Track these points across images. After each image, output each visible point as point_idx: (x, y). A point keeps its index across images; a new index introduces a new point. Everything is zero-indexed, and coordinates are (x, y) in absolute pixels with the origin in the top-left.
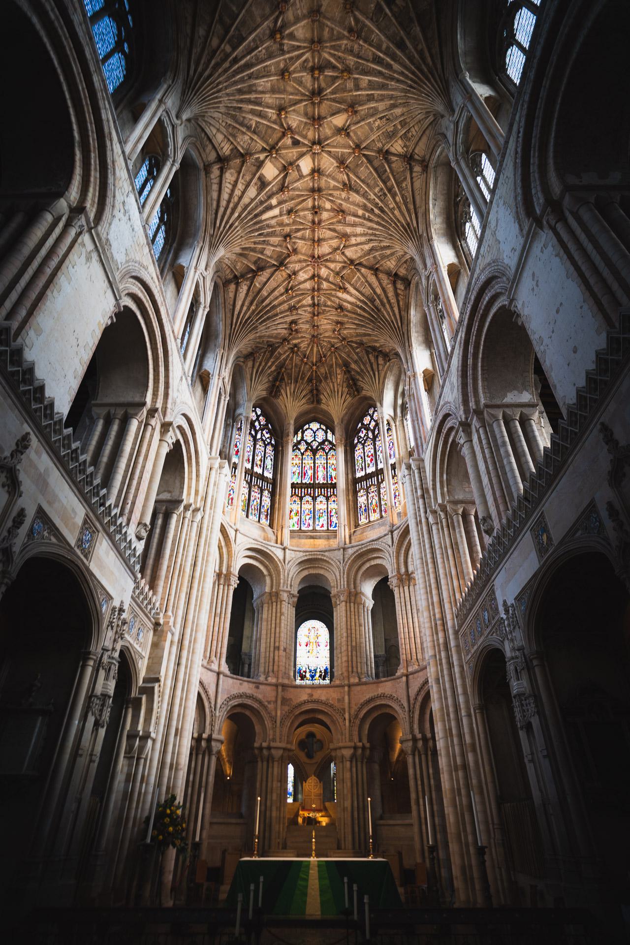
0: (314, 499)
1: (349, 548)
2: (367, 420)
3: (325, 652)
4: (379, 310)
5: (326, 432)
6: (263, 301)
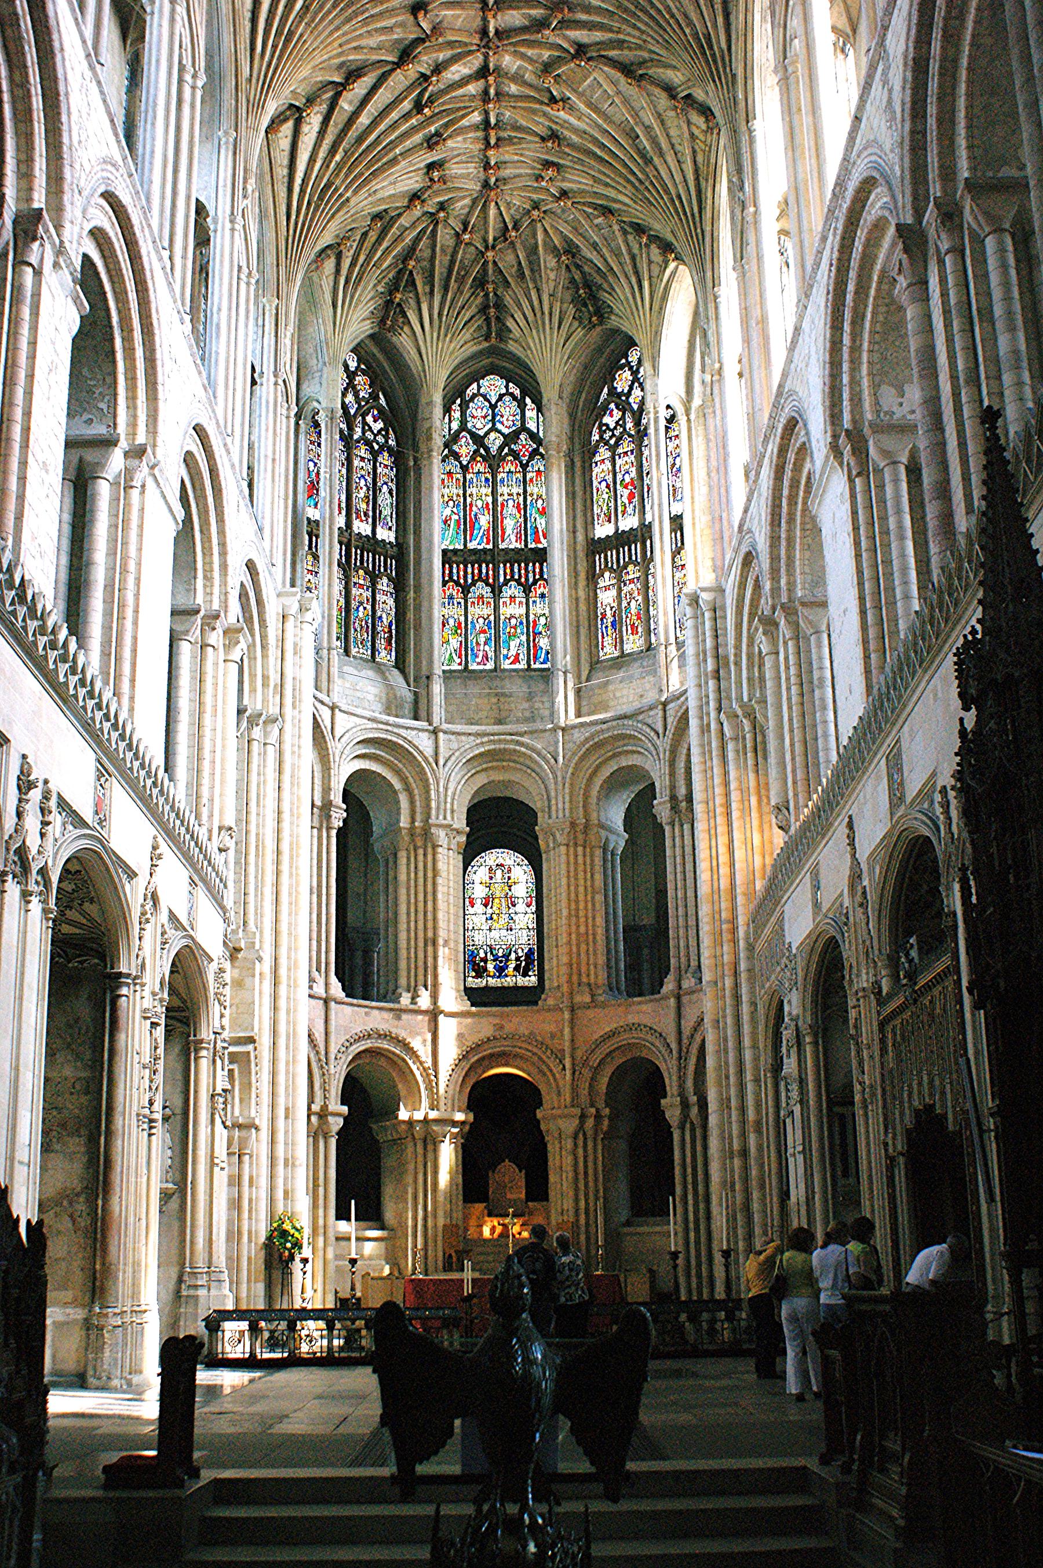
0: (496, 591)
1: (574, 727)
2: (623, 381)
3: (525, 917)
4: (648, 161)
5: (522, 406)
6: (360, 139)
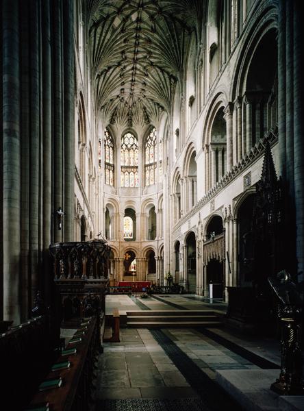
0: (129, 173)
2: (152, 135)
